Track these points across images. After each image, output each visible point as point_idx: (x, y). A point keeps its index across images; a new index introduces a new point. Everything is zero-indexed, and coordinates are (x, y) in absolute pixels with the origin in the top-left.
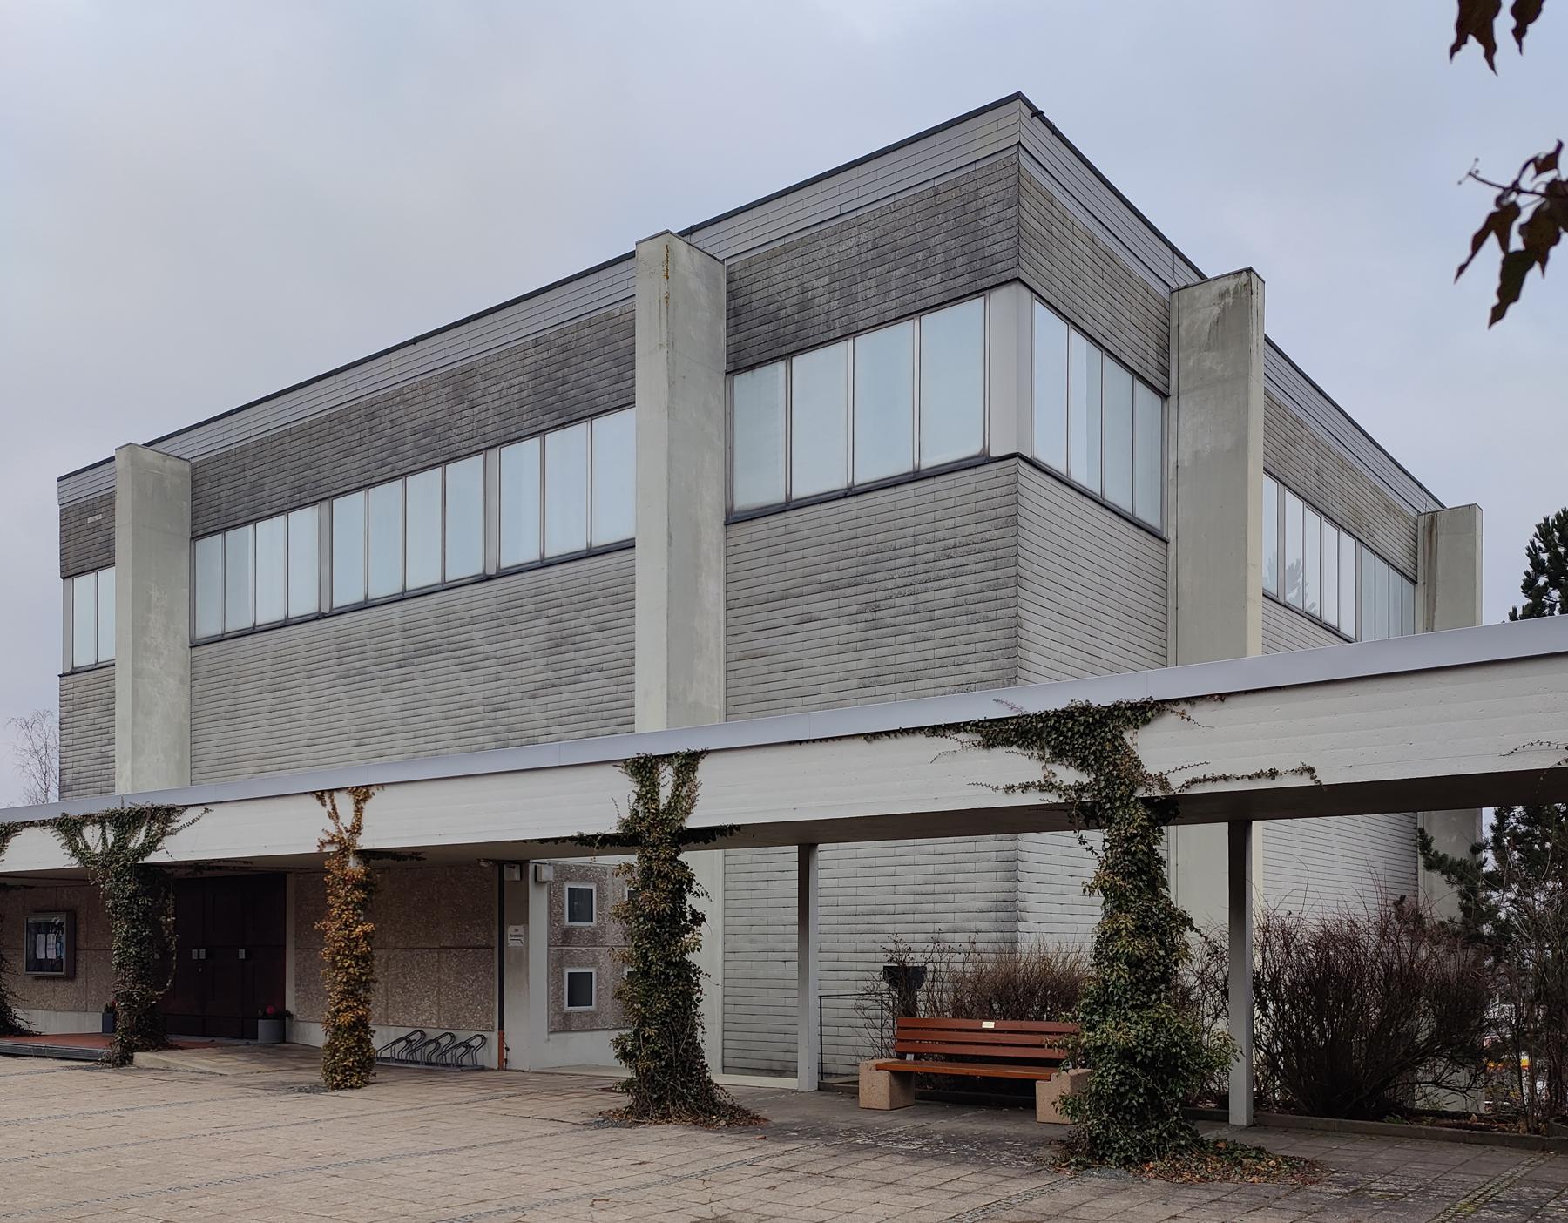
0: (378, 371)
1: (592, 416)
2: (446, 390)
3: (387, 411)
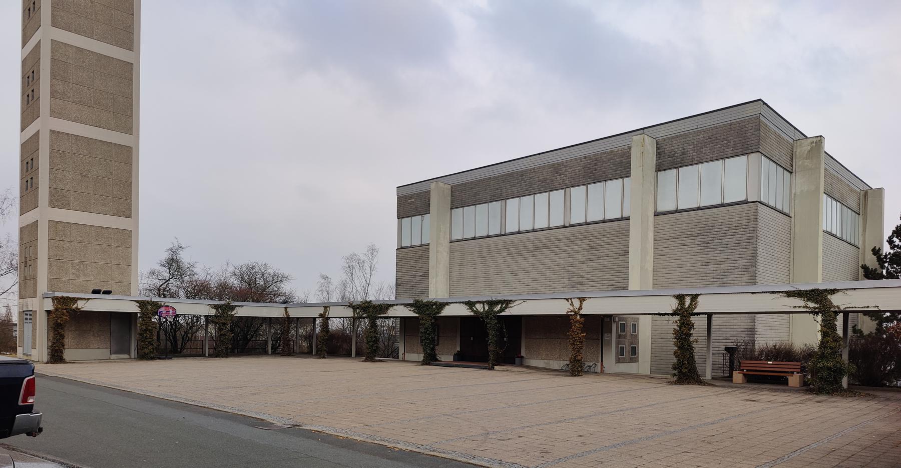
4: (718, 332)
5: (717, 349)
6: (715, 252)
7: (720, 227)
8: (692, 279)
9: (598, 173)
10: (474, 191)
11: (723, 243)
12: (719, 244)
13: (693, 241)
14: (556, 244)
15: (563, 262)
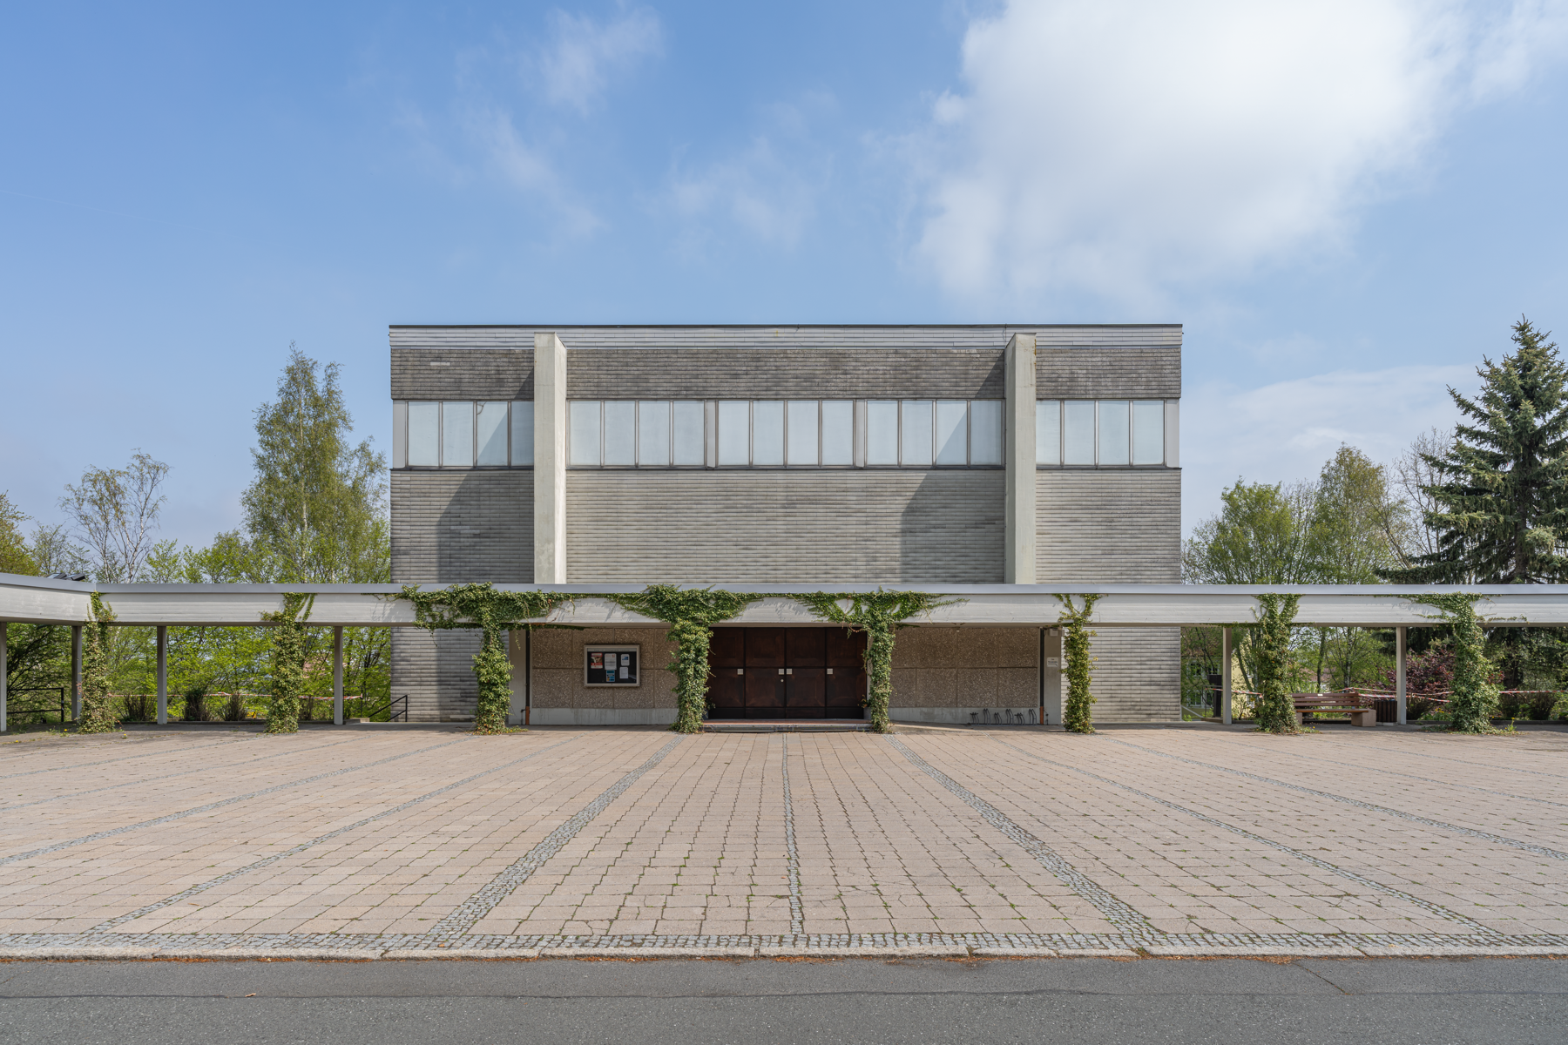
0: (765, 335)
1: (937, 399)
2: (824, 360)
3: (771, 360)
4: (1129, 655)
5: (1129, 679)
6: (1123, 536)
7: (1130, 499)
8: (1090, 573)
9: (923, 384)
10: (634, 371)
11: (1135, 524)
12: (1128, 523)
13: (1090, 516)
14: (838, 498)
15: (854, 531)
